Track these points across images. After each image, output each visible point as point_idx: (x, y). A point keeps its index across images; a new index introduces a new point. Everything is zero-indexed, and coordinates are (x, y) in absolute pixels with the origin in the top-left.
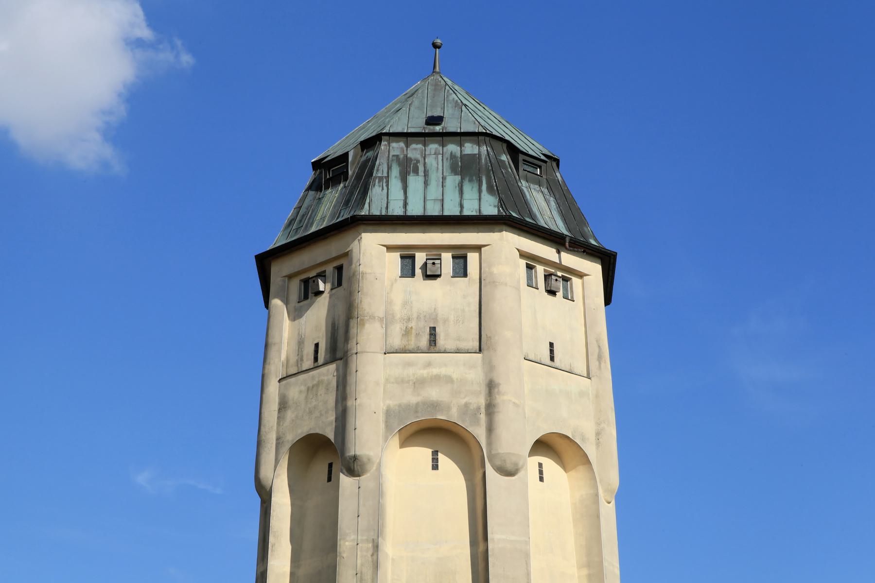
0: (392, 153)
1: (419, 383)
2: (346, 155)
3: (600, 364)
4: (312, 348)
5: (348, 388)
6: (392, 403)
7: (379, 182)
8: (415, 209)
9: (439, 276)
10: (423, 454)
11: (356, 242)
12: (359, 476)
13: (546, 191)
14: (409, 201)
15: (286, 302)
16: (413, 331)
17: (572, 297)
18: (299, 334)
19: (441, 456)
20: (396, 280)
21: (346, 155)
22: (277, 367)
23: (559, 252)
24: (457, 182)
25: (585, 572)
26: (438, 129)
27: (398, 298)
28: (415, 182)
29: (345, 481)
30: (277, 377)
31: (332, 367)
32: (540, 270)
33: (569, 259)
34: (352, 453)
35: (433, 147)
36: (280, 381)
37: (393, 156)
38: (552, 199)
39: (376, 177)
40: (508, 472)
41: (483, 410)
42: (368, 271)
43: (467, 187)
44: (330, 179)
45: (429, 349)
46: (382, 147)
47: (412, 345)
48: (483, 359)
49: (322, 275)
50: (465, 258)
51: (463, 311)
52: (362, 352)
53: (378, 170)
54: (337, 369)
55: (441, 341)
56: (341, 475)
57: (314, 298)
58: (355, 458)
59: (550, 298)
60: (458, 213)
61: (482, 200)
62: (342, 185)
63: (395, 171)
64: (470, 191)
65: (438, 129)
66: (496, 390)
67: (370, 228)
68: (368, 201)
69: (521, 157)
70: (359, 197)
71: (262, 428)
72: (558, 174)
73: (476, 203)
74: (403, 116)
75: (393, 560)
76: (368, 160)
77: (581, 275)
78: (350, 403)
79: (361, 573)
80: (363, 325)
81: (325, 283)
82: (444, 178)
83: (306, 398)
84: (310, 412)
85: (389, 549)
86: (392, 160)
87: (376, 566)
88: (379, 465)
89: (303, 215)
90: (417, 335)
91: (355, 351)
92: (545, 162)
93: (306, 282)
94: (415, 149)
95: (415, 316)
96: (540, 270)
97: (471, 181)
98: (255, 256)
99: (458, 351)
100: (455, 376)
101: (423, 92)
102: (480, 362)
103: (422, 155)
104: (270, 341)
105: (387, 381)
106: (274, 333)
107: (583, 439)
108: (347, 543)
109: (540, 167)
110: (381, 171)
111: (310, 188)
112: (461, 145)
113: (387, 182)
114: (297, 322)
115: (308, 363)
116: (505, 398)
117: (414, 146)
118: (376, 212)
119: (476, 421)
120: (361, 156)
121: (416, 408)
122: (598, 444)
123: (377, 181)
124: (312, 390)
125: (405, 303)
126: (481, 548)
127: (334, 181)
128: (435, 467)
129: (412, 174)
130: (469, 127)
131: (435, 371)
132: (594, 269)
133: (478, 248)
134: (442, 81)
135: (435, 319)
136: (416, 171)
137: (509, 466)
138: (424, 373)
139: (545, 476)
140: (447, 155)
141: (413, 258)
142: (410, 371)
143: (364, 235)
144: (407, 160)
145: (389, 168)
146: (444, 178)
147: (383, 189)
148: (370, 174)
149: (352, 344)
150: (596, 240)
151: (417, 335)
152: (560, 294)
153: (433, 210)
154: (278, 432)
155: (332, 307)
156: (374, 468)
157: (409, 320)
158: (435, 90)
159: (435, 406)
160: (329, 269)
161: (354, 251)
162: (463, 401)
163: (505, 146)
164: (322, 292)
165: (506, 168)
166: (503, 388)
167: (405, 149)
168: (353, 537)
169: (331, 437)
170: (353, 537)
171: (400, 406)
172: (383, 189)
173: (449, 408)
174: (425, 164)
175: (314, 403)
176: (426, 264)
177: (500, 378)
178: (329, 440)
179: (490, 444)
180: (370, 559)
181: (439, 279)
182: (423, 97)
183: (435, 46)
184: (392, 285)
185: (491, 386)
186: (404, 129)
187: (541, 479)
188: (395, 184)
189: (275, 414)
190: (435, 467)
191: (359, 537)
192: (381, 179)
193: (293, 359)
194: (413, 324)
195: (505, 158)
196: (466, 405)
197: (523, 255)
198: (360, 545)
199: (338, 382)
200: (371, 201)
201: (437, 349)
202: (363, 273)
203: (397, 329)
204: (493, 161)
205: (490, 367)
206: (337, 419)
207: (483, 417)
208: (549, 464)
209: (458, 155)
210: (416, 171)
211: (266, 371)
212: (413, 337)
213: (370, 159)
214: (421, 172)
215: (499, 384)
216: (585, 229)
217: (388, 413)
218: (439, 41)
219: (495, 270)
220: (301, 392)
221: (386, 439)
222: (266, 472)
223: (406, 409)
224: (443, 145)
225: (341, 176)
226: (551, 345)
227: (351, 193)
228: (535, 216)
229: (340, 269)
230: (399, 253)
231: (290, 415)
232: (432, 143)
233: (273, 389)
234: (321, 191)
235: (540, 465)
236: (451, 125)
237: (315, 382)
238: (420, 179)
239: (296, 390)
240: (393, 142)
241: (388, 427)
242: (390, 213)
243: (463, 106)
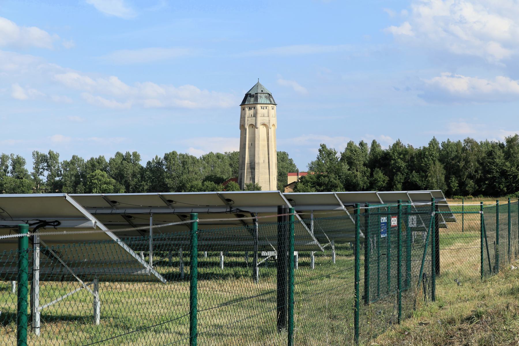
1: (263, 120)
8: (263, 103)
10: (262, 126)
35: (263, 94)
40: (270, 129)
115: (251, 116)
159: (264, 122)
185: (269, 120)
203: (261, 114)
205: (269, 119)
231: (249, 121)
236: (264, 92)
239: (249, 119)
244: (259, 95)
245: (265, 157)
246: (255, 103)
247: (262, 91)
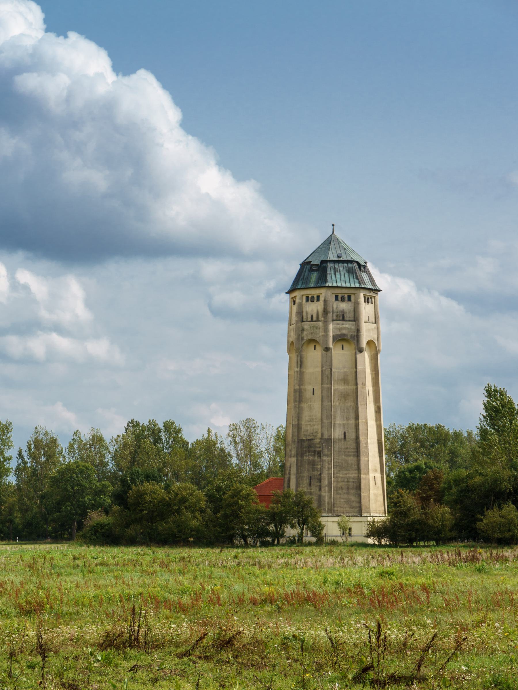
1: (341, 329)
4: (311, 316)
6: (334, 334)
26: (341, 259)
27: (335, 306)
35: (341, 265)
47: (338, 319)
55: (346, 318)
82: (344, 274)
90: (340, 316)
99: (349, 321)
115: (309, 319)
125: (336, 308)
131: (344, 326)
133: (354, 294)
135: (344, 313)
138: (341, 326)
141: (338, 296)
146: (344, 274)
157: (338, 312)
192: (329, 274)
194: (338, 314)
196: (352, 335)
203: (335, 314)
236: (344, 258)
238: (339, 274)
244: (330, 265)
246: (319, 285)
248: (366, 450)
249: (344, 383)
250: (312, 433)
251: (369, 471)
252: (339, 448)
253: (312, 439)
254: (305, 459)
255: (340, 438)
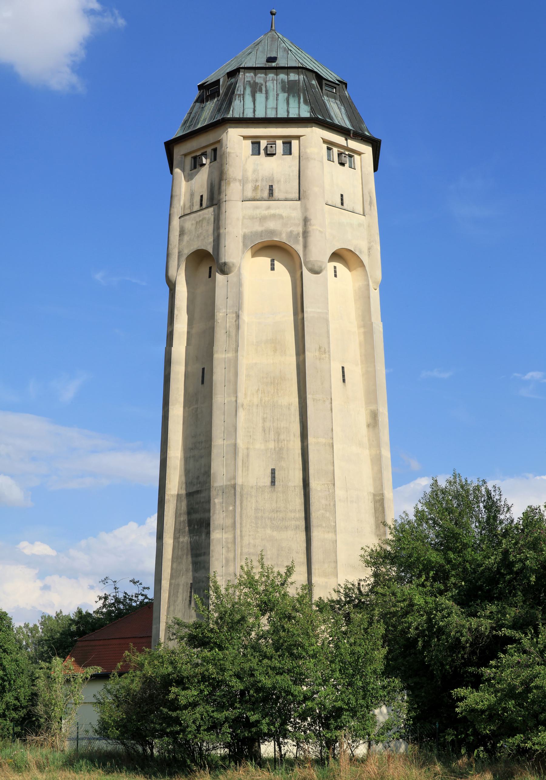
0: (246, 80)
1: (263, 219)
2: (218, 81)
3: (371, 207)
4: (199, 198)
5: (220, 222)
6: (247, 231)
7: (238, 97)
8: (260, 114)
9: (275, 154)
10: (265, 261)
11: (225, 134)
12: (227, 274)
13: (339, 102)
14: (257, 108)
15: (183, 170)
16: (259, 188)
17: (354, 167)
18: (191, 190)
19: (276, 262)
20: (249, 157)
21: (218, 81)
22: (177, 211)
23: (346, 140)
24: (285, 97)
25: (362, 330)
26: (274, 64)
27: (250, 168)
28: (260, 97)
29: (219, 277)
30: (178, 216)
31: (211, 209)
32: (335, 150)
33: (353, 144)
34: (223, 261)
35: (271, 76)
36: (180, 218)
37: (247, 81)
38: (342, 107)
39: (237, 94)
41: (301, 235)
42: (232, 151)
43: (291, 100)
44: (209, 95)
45: (269, 199)
46: (240, 76)
47: (259, 196)
48: (301, 204)
49: (204, 154)
50: (290, 143)
51: (289, 175)
52: (229, 201)
53: (238, 90)
54: (214, 211)
55: (276, 194)
56: (217, 274)
57: (200, 168)
58: (225, 264)
59: (341, 167)
60: (286, 117)
61: (300, 108)
62: (216, 99)
63: (248, 91)
64: (293, 103)
65: (274, 64)
66: (309, 223)
67: (233, 125)
68: (232, 109)
69: (324, 82)
70: (226, 106)
71: (170, 246)
72: (346, 92)
73: (297, 109)
74: (252, 56)
75: (247, 323)
76: (231, 84)
77: (359, 154)
78: (222, 231)
79: (229, 331)
80: (229, 184)
81: (206, 159)
82: (277, 95)
83: (196, 228)
84: (198, 237)
85: (245, 317)
86: (247, 84)
87: (238, 327)
88: (240, 268)
89: (193, 118)
90: (262, 190)
91: (225, 200)
92: (338, 85)
93: (195, 158)
94: (260, 77)
95: (260, 178)
96: (335, 150)
97: (294, 96)
98: (165, 143)
99: (286, 200)
100: (284, 215)
101: (264, 42)
102: (299, 206)
103: (264, 81)
104: (174, 194)
105: (244, 218)
106: (176, 190)
107: (361, 252)
108: (221, 314)
109: (335, 88)
110: (239, 90)
111: (197, 101)
112: (288, 75)
113: (243, 97)
114: (190, 182)
115: (197, 207)
116: (314, 227)
117: (259, 75)
118: (237, 116)
119: (297, 241)
120: (228, 82)
121: (261, 234)
122: (369, 255)
123: (237, 97)
124: (199, 223)
125: (254, 171)
126: (300, 317)
127: (211, 97)
128: (273, 269)
129: (258, 92)
130: (292, 63)
131: (272, 212)
132: (367, 150)
133: (298, 137)
134: (276, 35)
135: (273, 180)
136: (261, 91)
137: (316, 268)
138: (266, 213)
139: (338, 274)
140: (280, 81)
141: (259, 143)
142: (258, 212)
143: (229, 130)
144: (255, 84)
145: (245, 89)
146: (277, 95)
147: (241, 102)
148: (233, 92)
149: (223, 196)
150: (369, 132)
151: (262, 190)
152: (347, 165)
153: (271, 114)
154: (179, 249)
155: (210, 174)
156: (236, 270)
157: (257, 181)
158: (272, 41)
159: (272, 232)
160: (209, 150)
161: (224, 139)
162: (289, 230)
163: (314, 75)
164: (205, 164)
165: (315, 89)
166: (313, 221)
167: (254, 77)
168: (224, 310)
169: (211, 251)
170: (224, 310)
171: (251, 232)
172: (241, 102)
173: (280, 234)
174: (266, 86)
175: (200, 231)
176: (267, 147)
177: (311, 216)
178: (209, 253)
179: (305, 255)
180: (234, 323)
181: (274, 156)
182: (265, 45)
183: (272, 14)
184: (247, 159)
185: (306, 221)
186: (253, 65)
187: (336, 276)
188: (248, 98)
189: (177, 238)
190: (273, 269)
191: (228, 311)
192: (239, 95)
193: (188, 205)
194: (259, 183)
195: (314, 82)
196: (291, 232)
197: (325, 141)
198: (228, 315)
199: (214, 218)
200: (233, 109)
201: (273, 198)
202: (229, 153)
203: (249, 187)
204: (307, 84)
205: (305, 209)
206: (214, 240)
207: (301, 239)
208: (340, 267)
209: (286, 80)
210: (261, 91)
211: (172, 212)
212: (259, 191)
213: (233, 83)
214: (264, 91)
215: (310, 220)
216: (362, 125)
217: (245, 237)
218: (274, 11)
219: (308, 151)
220: (192, 224)
221: (243, 252)
222: (172, 272)
223: (255, 234)
224: (277, 75)
225: (215, 94)
226: (342, 196)
227: (222, 104)
228: (333, 118)
229: (215, 150)
230: (250, 141)
231: (186, 238)
232: (271, 73)
233: (176, 222)
234: (203, 103)
235: (335, 267)
236: (281, 62)
237: (201, 219)
238: (263, 95)
239: (189, 223)
240: (247, 73)
241: (245, 245)
242: (245, 116)
243: (289, 51)
245: (279, 453)
247: (271, 60)
248: (328, 514)
249: (275, 350)
250: (198, 477)
251: (336, 568)
252: (256, 510)
253: (198, 492)
254: (183, 542)
255: (261, 484)
